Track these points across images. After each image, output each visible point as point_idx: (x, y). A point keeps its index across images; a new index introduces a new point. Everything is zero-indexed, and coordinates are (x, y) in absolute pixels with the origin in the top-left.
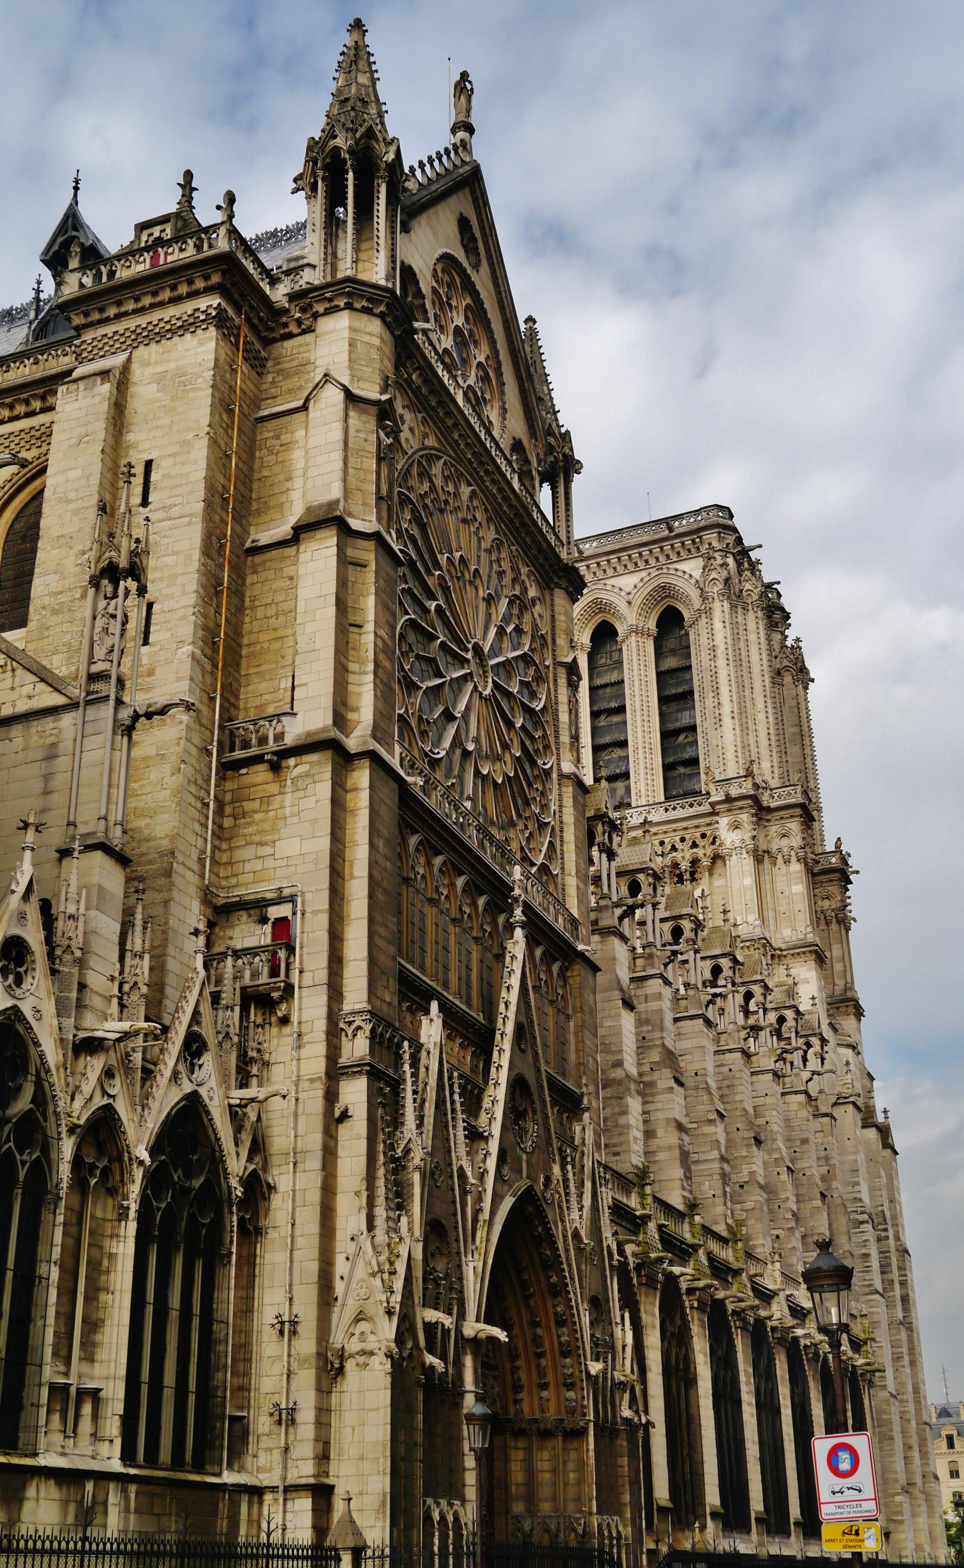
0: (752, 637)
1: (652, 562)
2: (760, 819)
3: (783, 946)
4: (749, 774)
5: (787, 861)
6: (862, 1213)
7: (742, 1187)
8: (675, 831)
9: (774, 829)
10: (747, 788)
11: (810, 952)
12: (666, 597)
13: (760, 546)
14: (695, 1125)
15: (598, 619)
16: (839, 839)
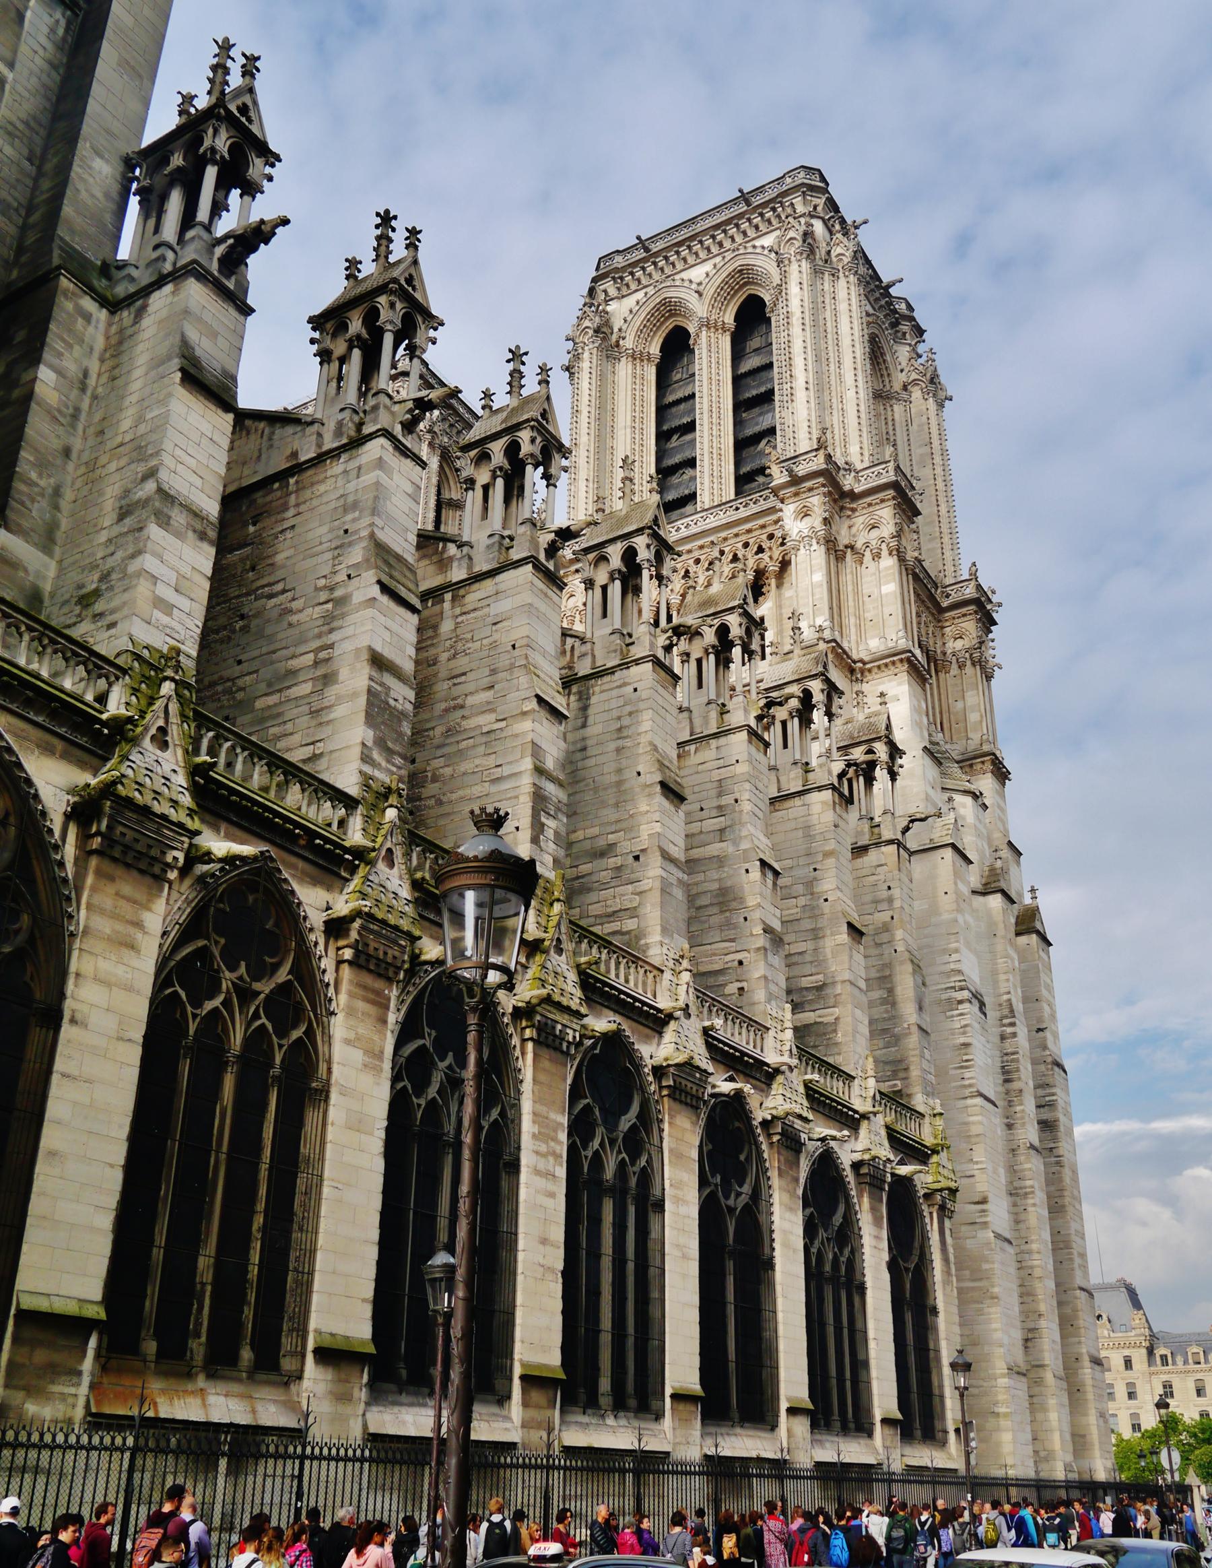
0: (843, 307)
1: (727, 244)
2: (842, 508)
3: (866, 659)
4: (821, 445)
5: (877, 556)
6: (962, 989)
7: (637, 858)
8: (736, 535)
9: (861, 519)
10: (819, 463)
11: (901, 660)
12: (746, 284)
13: (901, 281)
14: (503, 724)
15: (669, 325)
16: (974, 564)
